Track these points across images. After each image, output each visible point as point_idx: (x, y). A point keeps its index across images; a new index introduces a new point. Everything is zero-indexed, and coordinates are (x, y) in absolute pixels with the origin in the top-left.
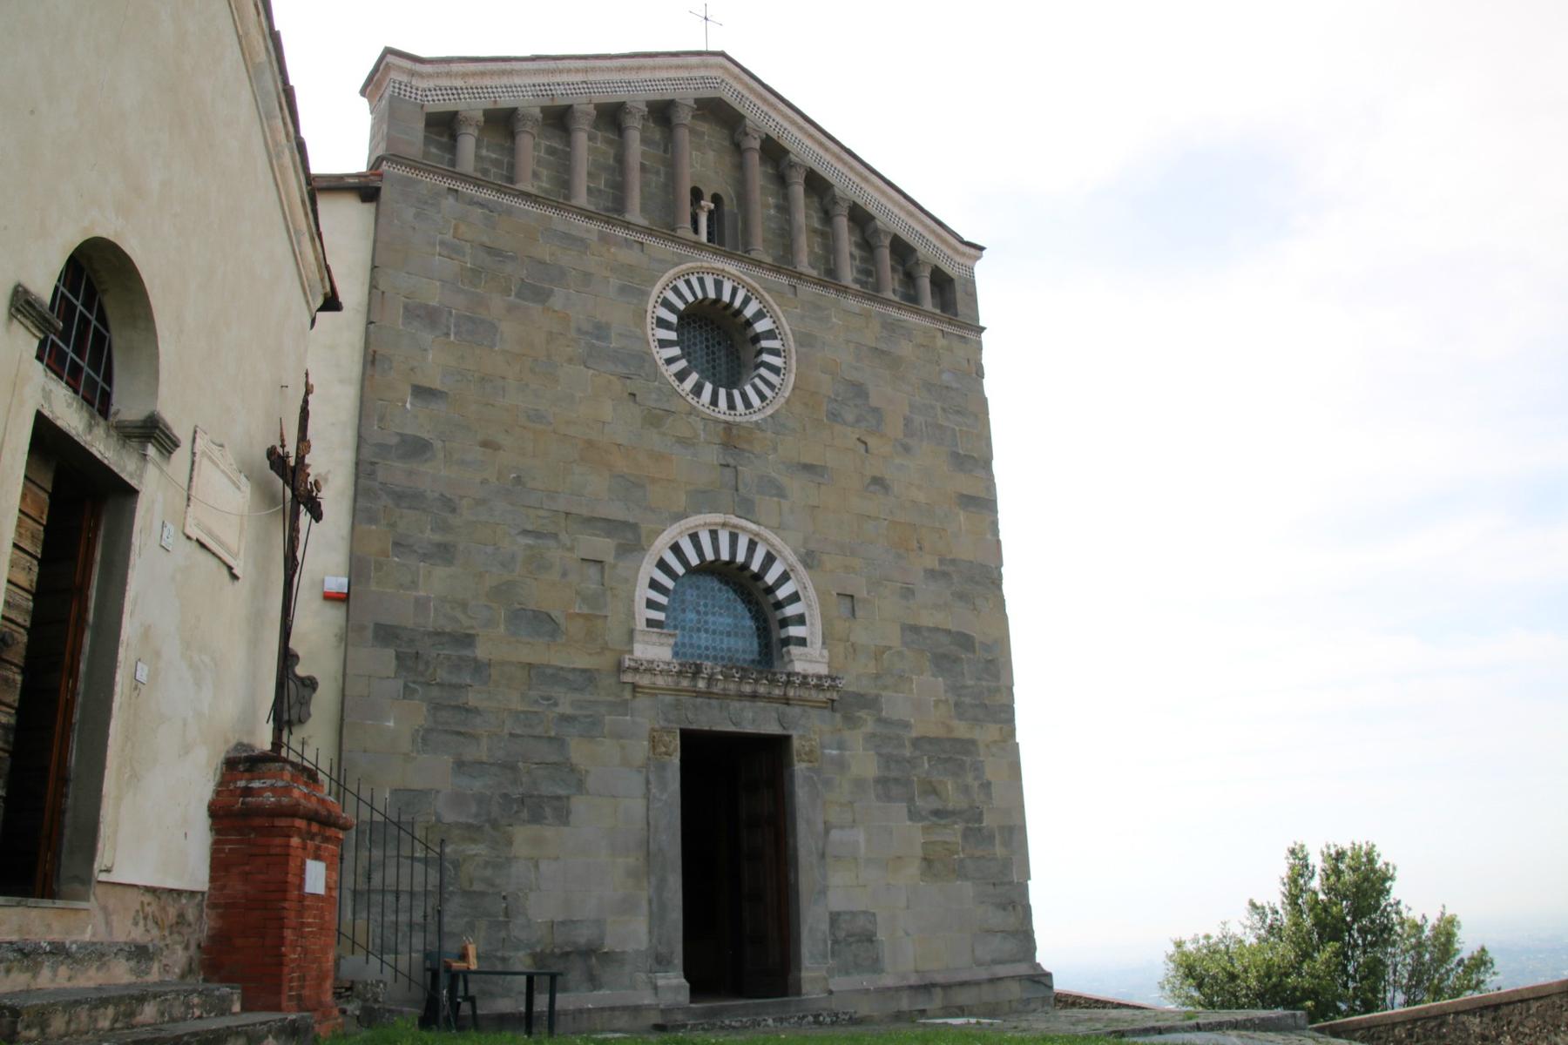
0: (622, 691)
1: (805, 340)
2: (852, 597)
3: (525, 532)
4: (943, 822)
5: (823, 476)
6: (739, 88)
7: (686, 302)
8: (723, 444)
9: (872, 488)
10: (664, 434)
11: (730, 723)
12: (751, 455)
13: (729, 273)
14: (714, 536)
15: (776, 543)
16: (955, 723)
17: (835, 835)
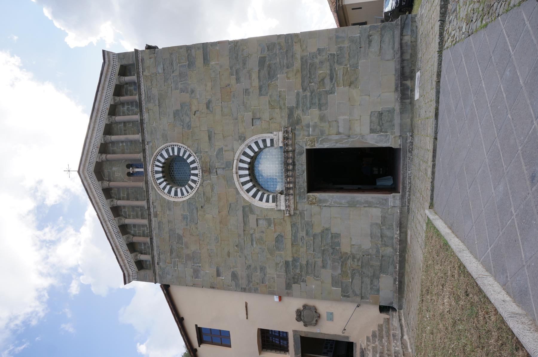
1: (165, 139)
2: (252, 119)
3: (252, 244)
4: (335, 76)
5: (211, 132)
6: (87, 164)
7: (167, 184)
8: (210, 174)
9: (211, 109)
10: (212, 196)
11: (304, 174)
12: (211, 161)
13: (152, 169)
14: (241, 176)
15: (239, 153)
16: (295, 68)
17: (341, 130)
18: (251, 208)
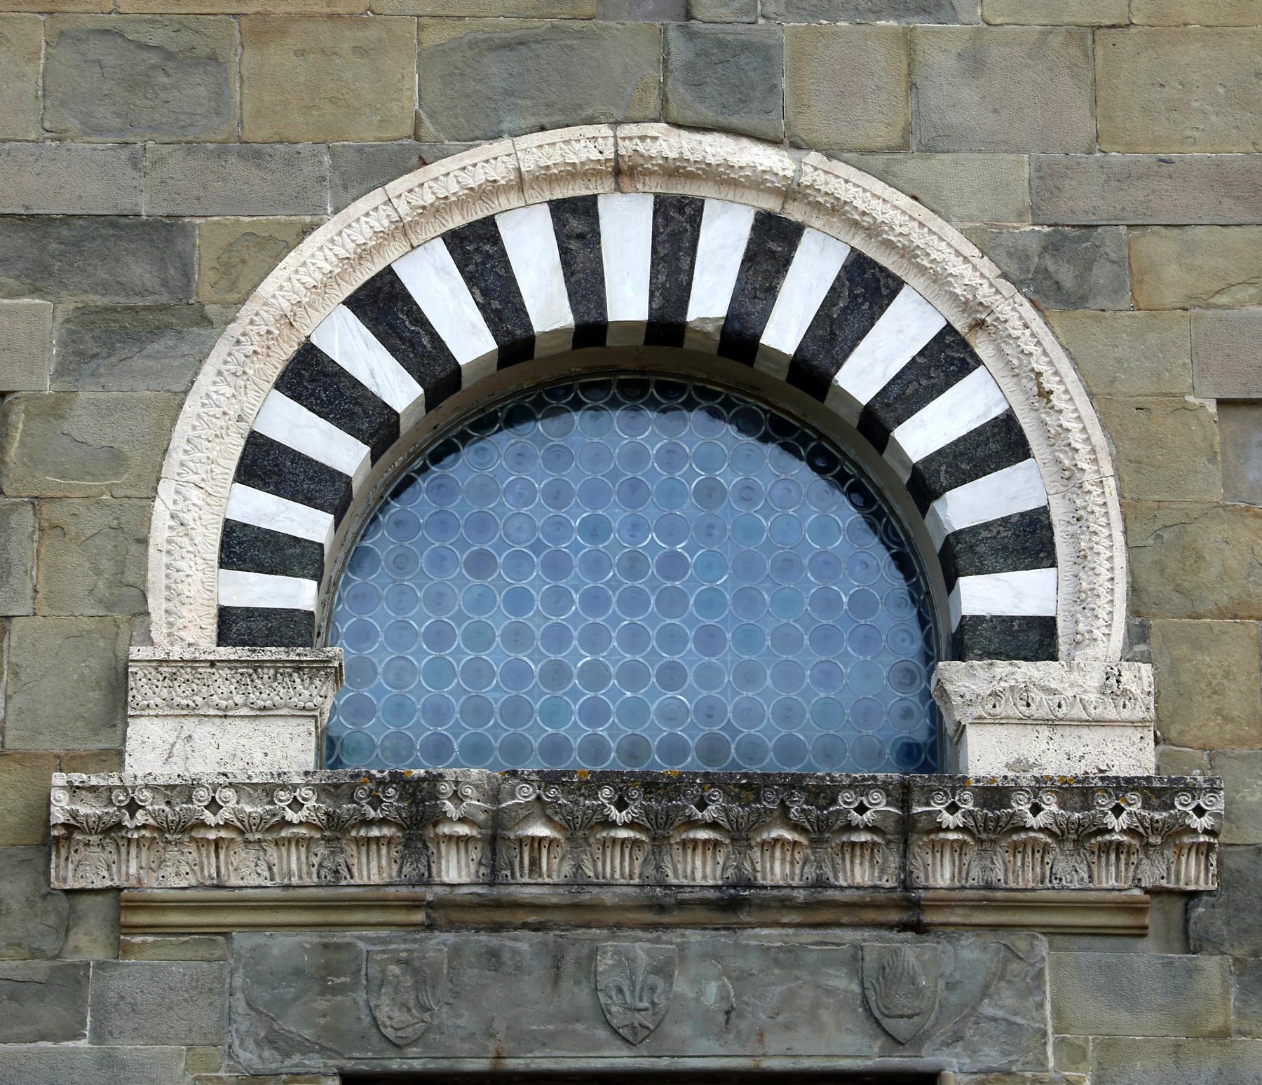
0: (66, 928)
11: (602, 1033)
14: (576, 225)
15: (879, 211)
18: (157, 331)
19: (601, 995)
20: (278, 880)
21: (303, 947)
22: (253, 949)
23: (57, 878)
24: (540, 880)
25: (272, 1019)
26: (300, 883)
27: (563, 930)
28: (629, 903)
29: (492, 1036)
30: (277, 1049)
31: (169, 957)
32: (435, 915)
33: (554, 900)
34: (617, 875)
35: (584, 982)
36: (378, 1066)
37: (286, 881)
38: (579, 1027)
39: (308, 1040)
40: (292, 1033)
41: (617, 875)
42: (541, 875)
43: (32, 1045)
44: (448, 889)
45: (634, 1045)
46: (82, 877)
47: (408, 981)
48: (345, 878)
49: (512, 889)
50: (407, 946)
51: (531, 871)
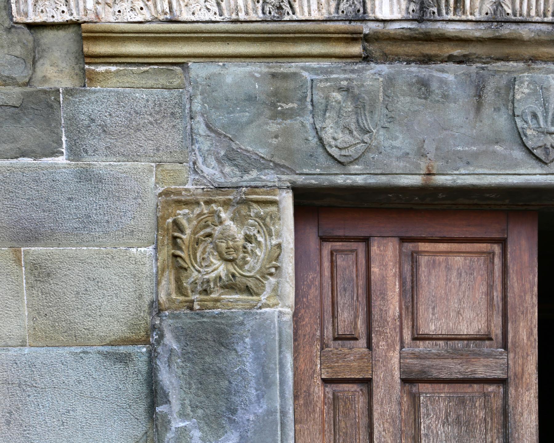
11: (518, 154)
19: (518, 120)
20: (226, 15)
21: (253, 76)
22: (209, 78)
23: (18, 12)
24: (464, 17)
25: (230, 139)
26: (247, 18)
27: (485, 63)
28: (543, 37)
29: (424, 155)
30: (236, 165)
31: (133, 85)
32: (371, 48)
33: (478, 34)
34: (533, 13)
35: (503, 109)
36: (325, 181)
37: (234, 17)
38: (498, 148)
39: (263, 158)
40: (249, 152)
41: (533, 13)
42: (464, 13)
43: (14, 161)
44: (381, 25)
45: (546, 164)
46: (42, 12)
47: (349, 107)
48: (288, 13)
49: (439, 25)
50: (346, 76)
51: (455, 9)
